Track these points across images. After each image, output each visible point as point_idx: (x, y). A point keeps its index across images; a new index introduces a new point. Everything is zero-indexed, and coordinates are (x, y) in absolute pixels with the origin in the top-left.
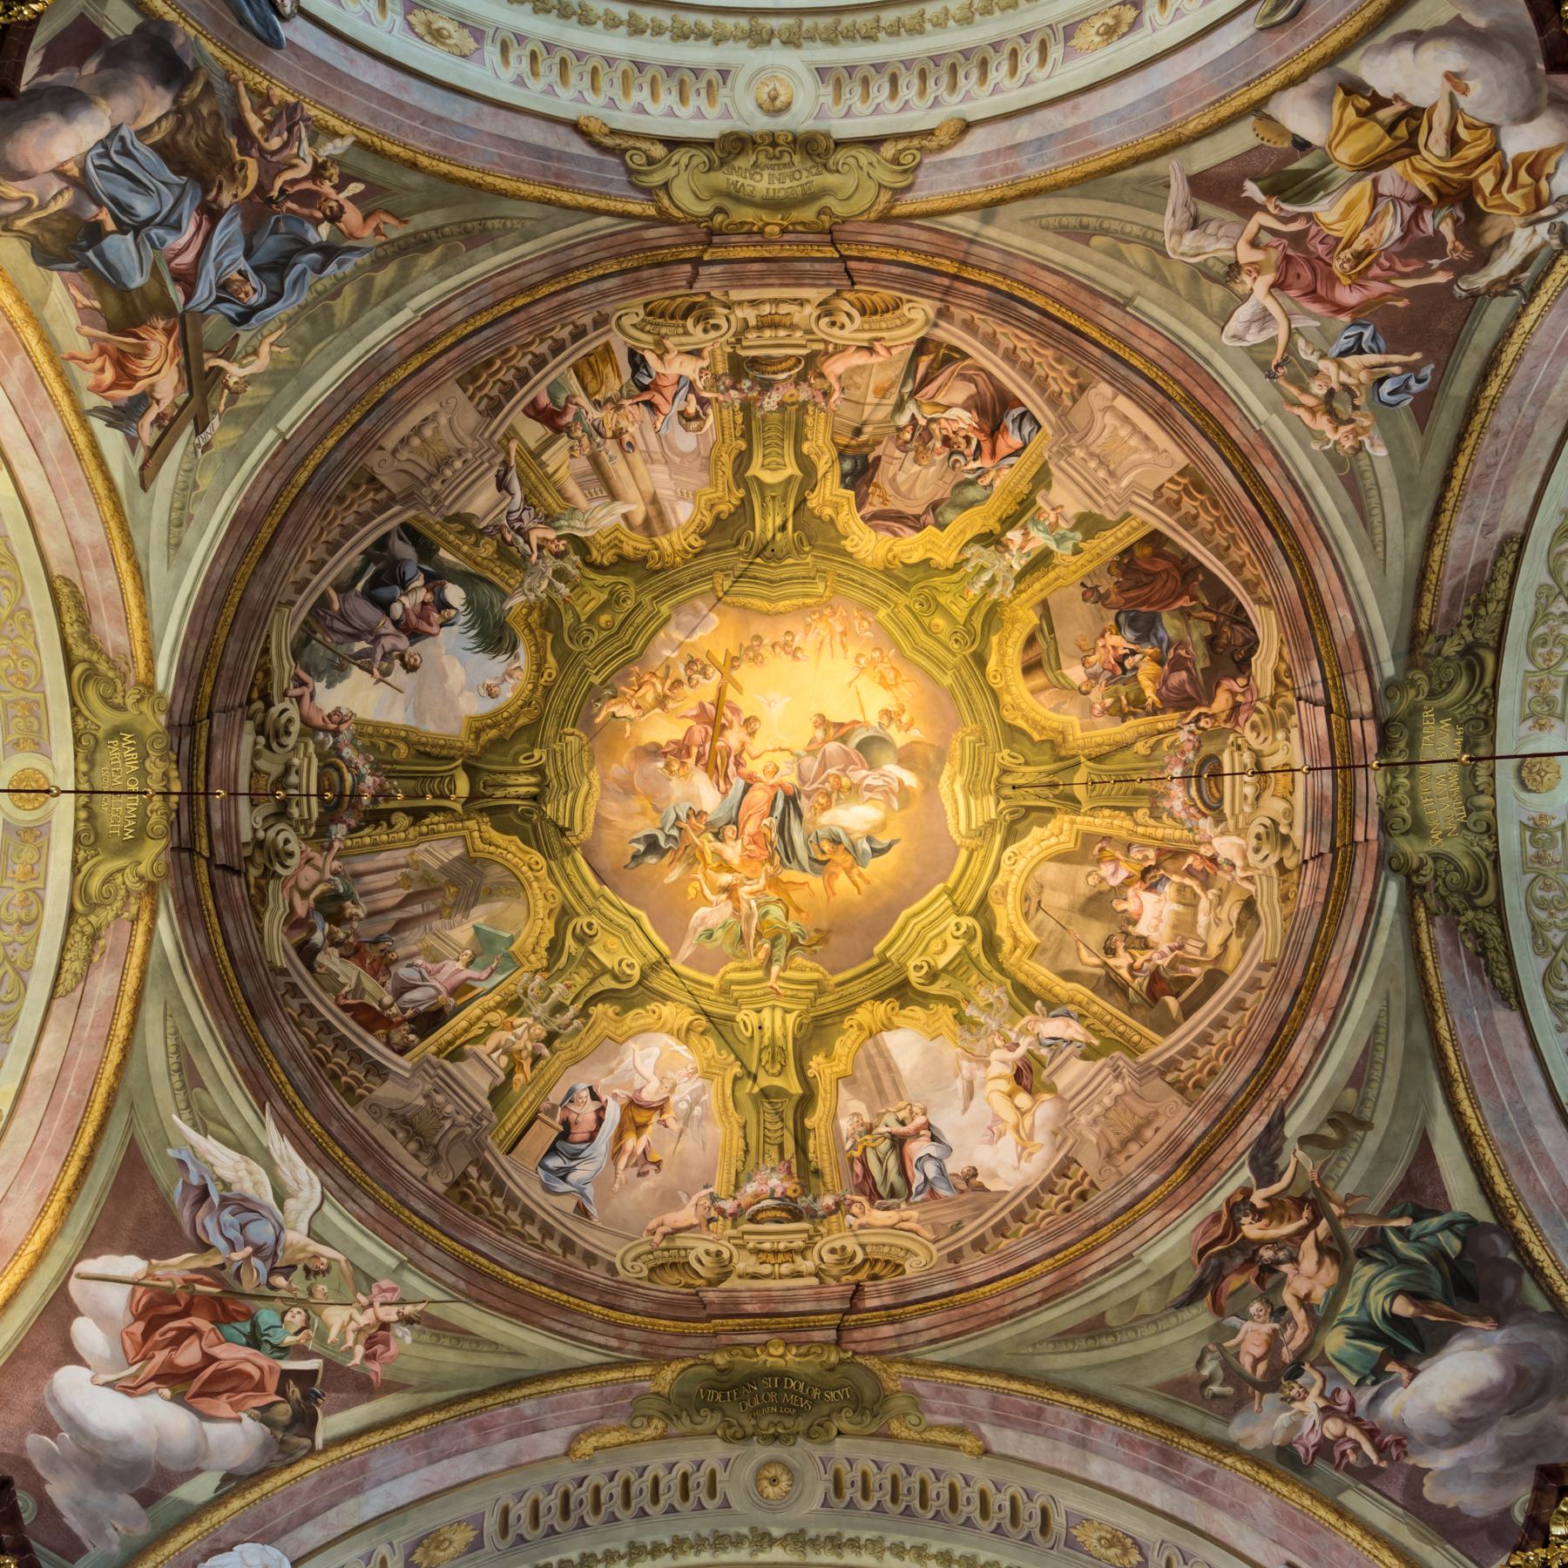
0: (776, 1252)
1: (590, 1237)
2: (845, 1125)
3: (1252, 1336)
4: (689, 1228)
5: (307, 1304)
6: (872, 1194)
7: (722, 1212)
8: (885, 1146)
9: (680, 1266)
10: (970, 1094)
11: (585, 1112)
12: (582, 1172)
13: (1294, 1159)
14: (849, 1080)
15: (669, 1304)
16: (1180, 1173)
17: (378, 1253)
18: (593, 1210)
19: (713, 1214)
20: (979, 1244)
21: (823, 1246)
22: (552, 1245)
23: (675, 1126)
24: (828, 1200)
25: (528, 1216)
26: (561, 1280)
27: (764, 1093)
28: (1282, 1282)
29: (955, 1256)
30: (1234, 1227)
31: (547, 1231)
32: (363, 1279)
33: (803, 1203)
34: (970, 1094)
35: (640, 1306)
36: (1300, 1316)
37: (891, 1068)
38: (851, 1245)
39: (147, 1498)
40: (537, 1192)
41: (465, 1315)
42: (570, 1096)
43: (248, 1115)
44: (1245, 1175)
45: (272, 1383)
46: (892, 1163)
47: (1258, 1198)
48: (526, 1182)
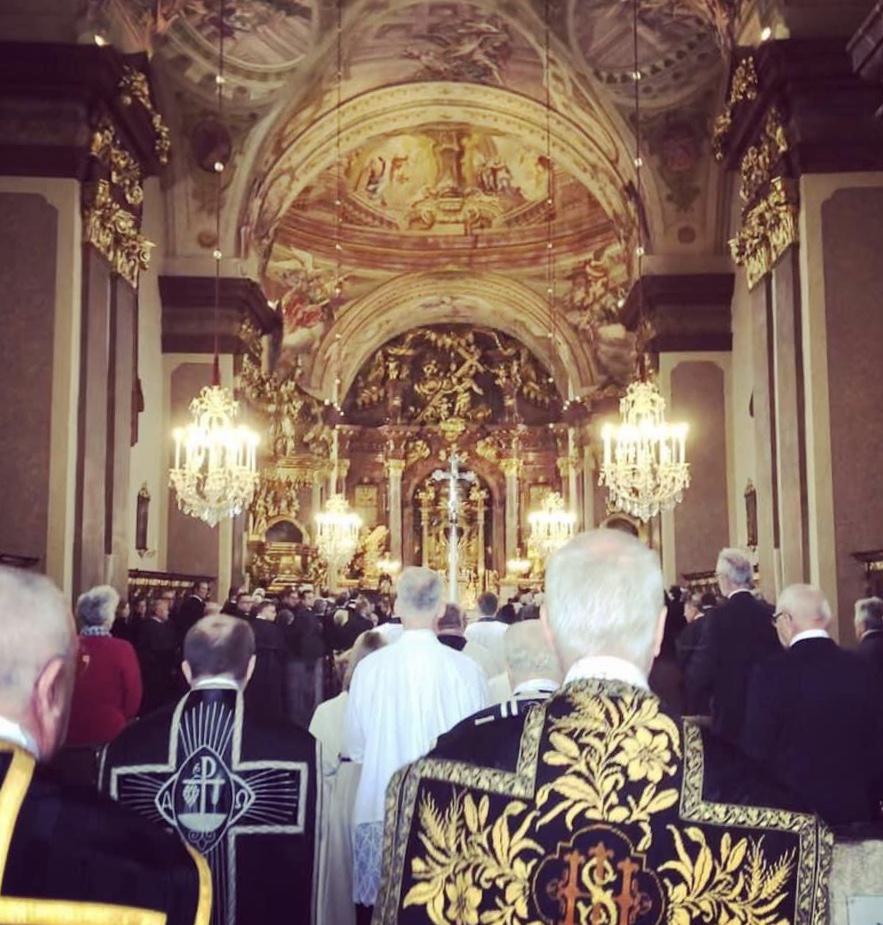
0: (450, 211)
1: (389, 214)
2: (476, 163)
3: (579, 295)
4: (420, 201)
5: (320, 286)
6: (482, 185)
7: (431, 194)
8: (489, 172)
9: (418, 219)
10: (522, 160)
11: (378, 166)
12: (381, 188)
13: (604, 261)
14: (477, 147)
15: (416, 244)
16: (577, 237)
17: (332, 264)
18: (386, 201)
19: (428, 195)
20: (517, 219)
21: (466, 208)
22: (377, 223)
23: (411, 164)
24: (468, 190)
25: (367, 213)
26: (387, 243)
27: (446, 151)
28: (591, 286)
29: (508, 223)
30: (584, 267)
31: (374, 217)
32: (331, 273)
33: (460, 190)
34: (522, 160)
35: (409, 247)
36: (591, 296)
37: (494, 147)
38: (476, 209)
39: (309, 353)
40: (366, 200)
41: (361, 272)
42: (372, 162)
43: (287, 251)
44: (590, 256)
45: (320, 311)
46: (491, 178)
47: (593, 263)
48: (361, 197)
